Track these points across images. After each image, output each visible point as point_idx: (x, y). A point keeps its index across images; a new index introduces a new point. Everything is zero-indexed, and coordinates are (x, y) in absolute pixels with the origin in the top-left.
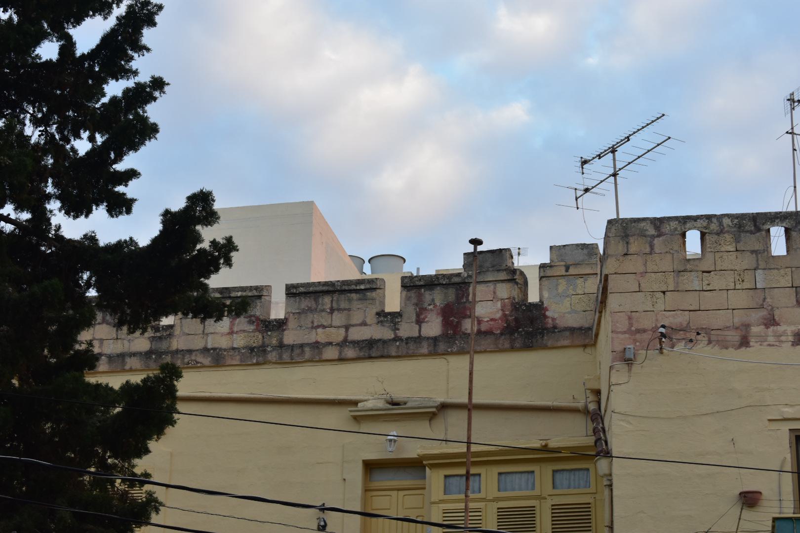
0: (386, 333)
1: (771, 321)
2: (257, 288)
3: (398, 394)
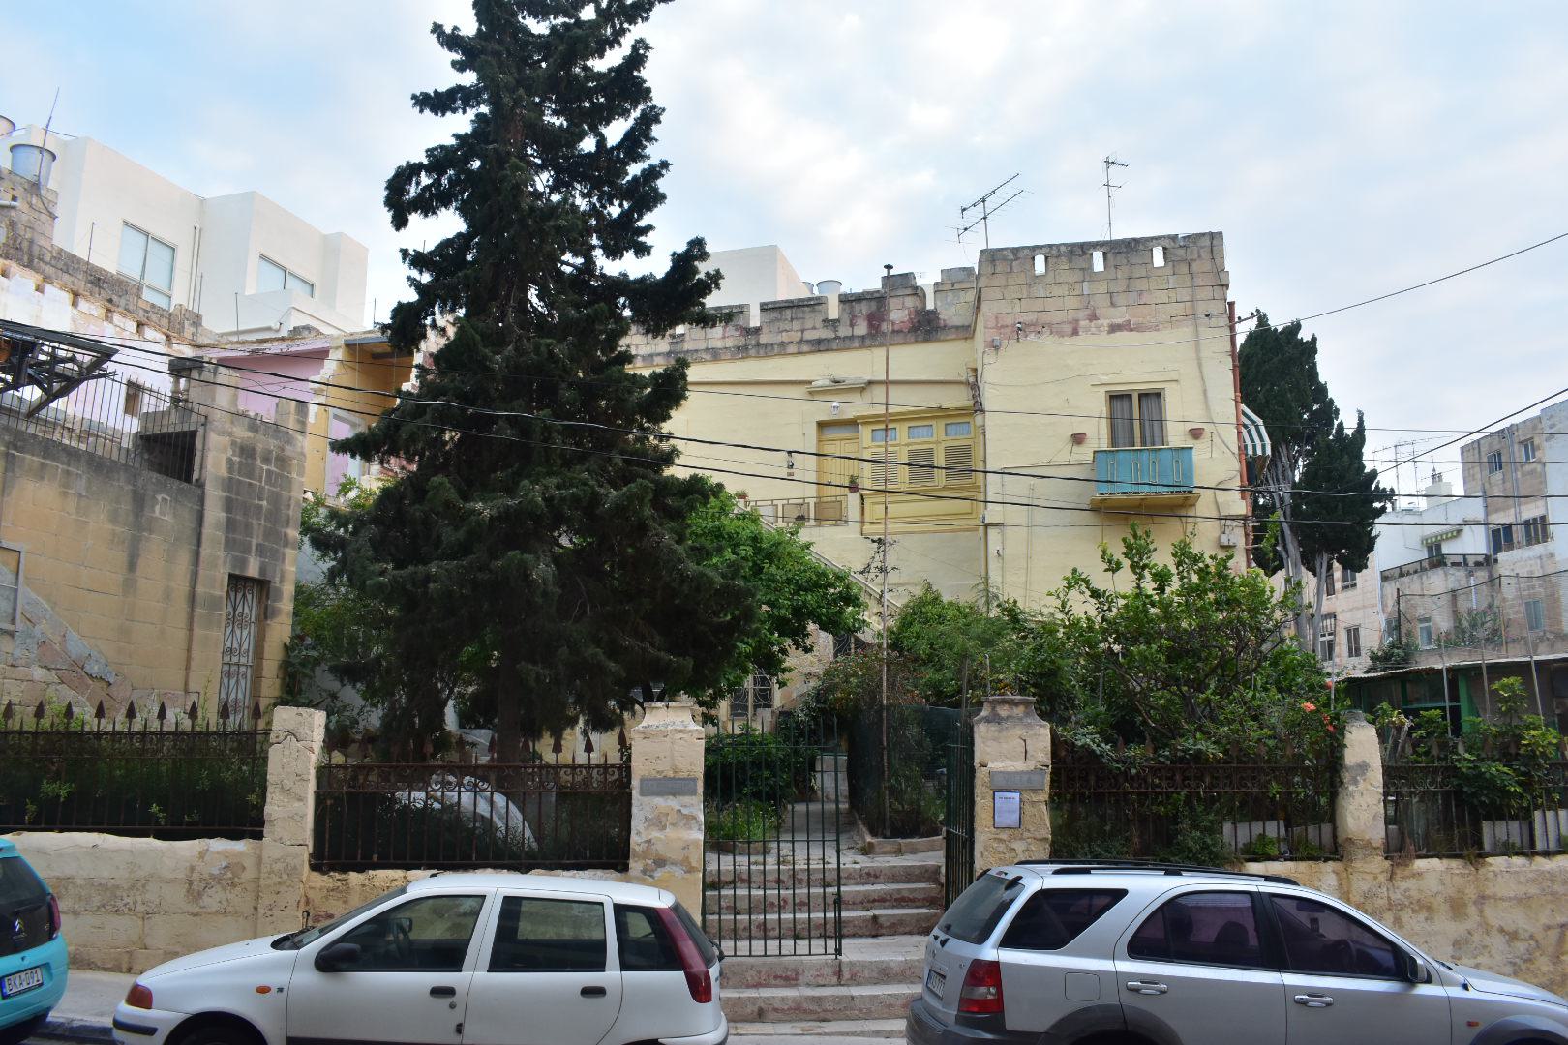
0: (828, 334)
1: (1093, 317)
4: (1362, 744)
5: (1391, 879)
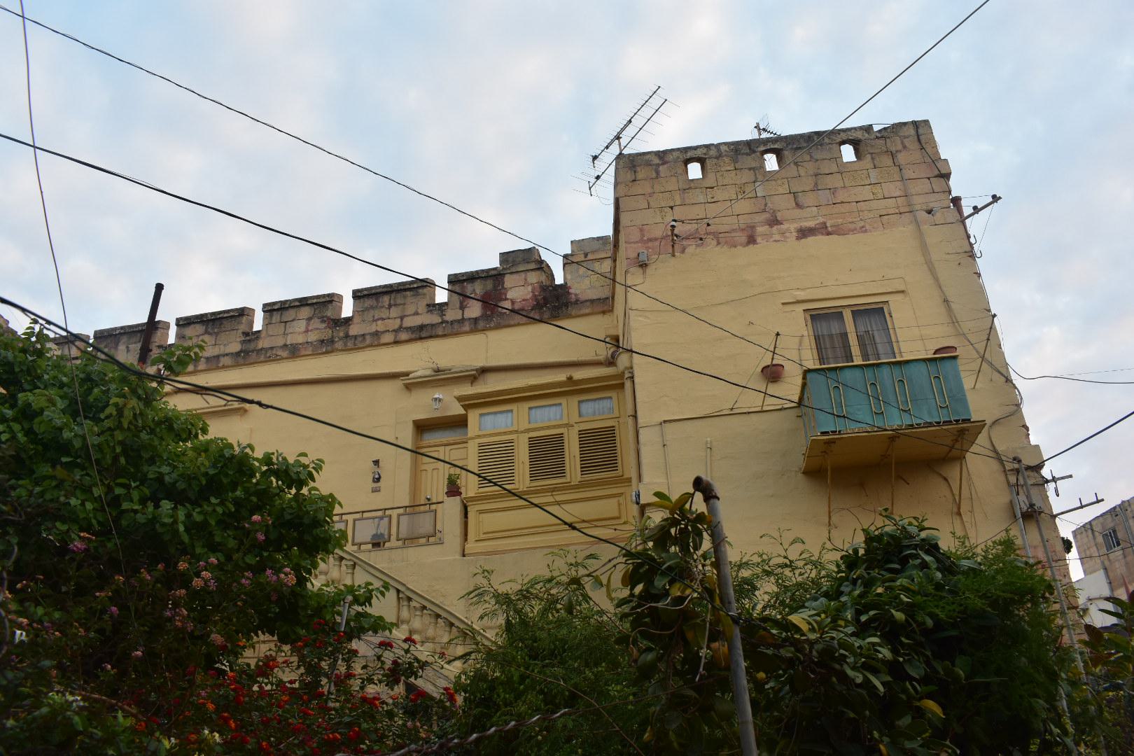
0: (435, 319)
1: (774, 222)
2: (329, 295)
3: (443, 364)
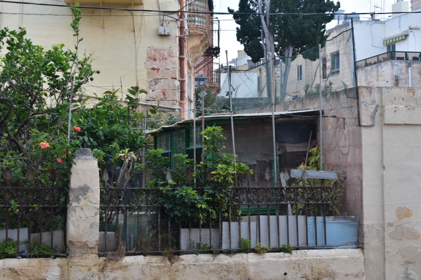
4: (86, 172)
5: (102, 270)
